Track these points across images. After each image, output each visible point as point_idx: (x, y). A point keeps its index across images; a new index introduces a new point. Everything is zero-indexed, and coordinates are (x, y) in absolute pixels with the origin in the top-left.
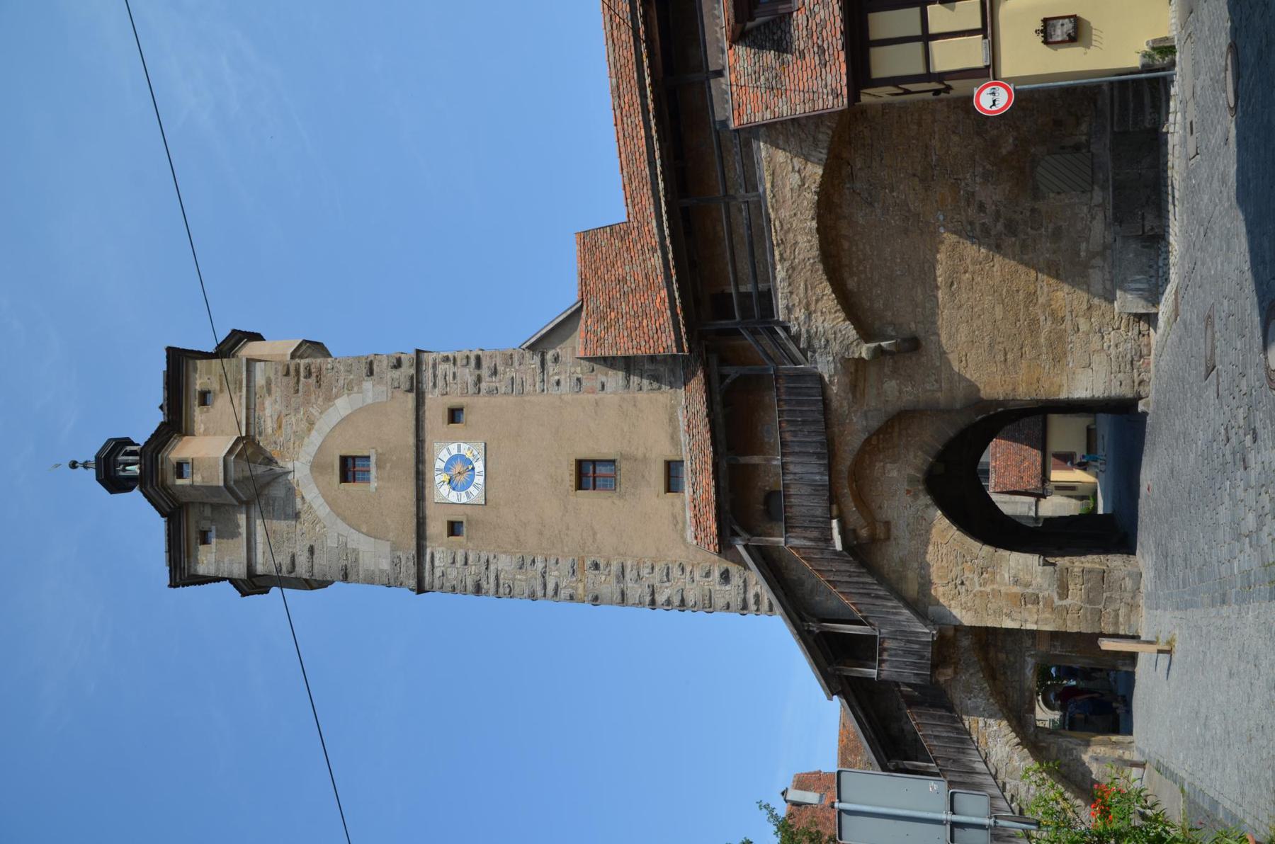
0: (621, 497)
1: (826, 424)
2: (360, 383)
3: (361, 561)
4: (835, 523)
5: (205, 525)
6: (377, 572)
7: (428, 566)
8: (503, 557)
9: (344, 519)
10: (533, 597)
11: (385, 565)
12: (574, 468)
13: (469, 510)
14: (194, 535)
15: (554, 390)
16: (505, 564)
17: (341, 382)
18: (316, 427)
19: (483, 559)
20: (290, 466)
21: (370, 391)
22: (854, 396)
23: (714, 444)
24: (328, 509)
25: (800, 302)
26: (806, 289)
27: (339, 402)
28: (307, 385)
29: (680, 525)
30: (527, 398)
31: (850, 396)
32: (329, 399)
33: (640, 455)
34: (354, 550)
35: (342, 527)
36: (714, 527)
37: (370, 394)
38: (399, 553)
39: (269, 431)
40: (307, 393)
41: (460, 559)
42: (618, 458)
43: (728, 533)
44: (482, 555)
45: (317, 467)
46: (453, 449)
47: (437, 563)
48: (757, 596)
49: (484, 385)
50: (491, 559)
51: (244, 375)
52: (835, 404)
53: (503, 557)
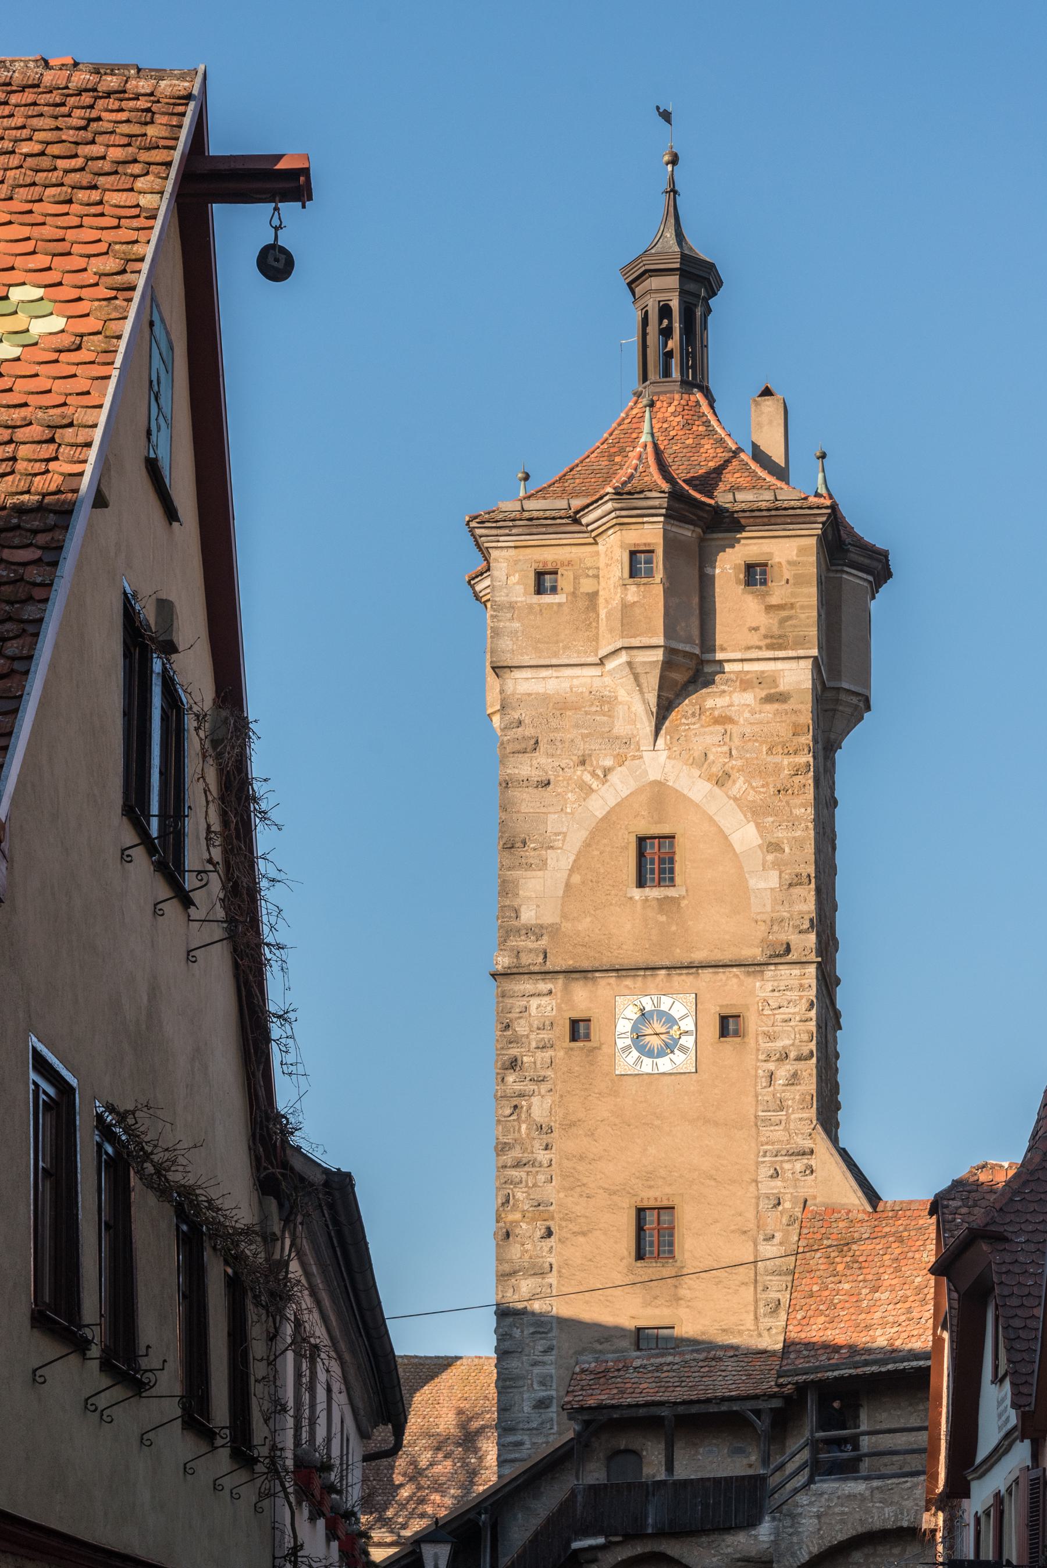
0: (631, 1271)
1: (709, 1530)
2: (777, 865)
3: (529, 874)
4: (601, 1540)
5: (565, 582)
6: (515, 904)
7: (527, 986)
8: (549, 1100)
9: (587, 845)
10: (502, 1148)
11: (528, 916)
12: (665, 1203)
13: (605, 1049)
14: (549, 556)
15: (765, 1172)
16: (539, 1108)
17: (781, 834)
18: (716, 789)
19: (543, 1073)
20: (660, 741)
21: (765, 883)
22: (738, 1560)
23: (683, 1403)
24: (600, 814)
25: (829, 1507)
26: (843, 1513)
27: (751, 829)
28: (778, 768)
29: (599, 1347)
30: (754, 1129)
31: (738, 1556)
32: (756, 812)
33: (683, 1292)
34: (544, 862)
35: (577, 838)
36: (591, 1402)
37: (762, 885)
38: (545, 937)
39: (709, 703)
40: (762, 772)
41: (545, 1035)
42: (678, 1264)
43: (586, 1417)
44: (549, 1073)
45: (660, 794)
46: (688, 1024)
47: (534, 1002)
48: (520, 1444)
49: (771, 1066)
50: (544, 1088)
51: (791, 653)
52: (730, 1539)
53: (549, 1100)
